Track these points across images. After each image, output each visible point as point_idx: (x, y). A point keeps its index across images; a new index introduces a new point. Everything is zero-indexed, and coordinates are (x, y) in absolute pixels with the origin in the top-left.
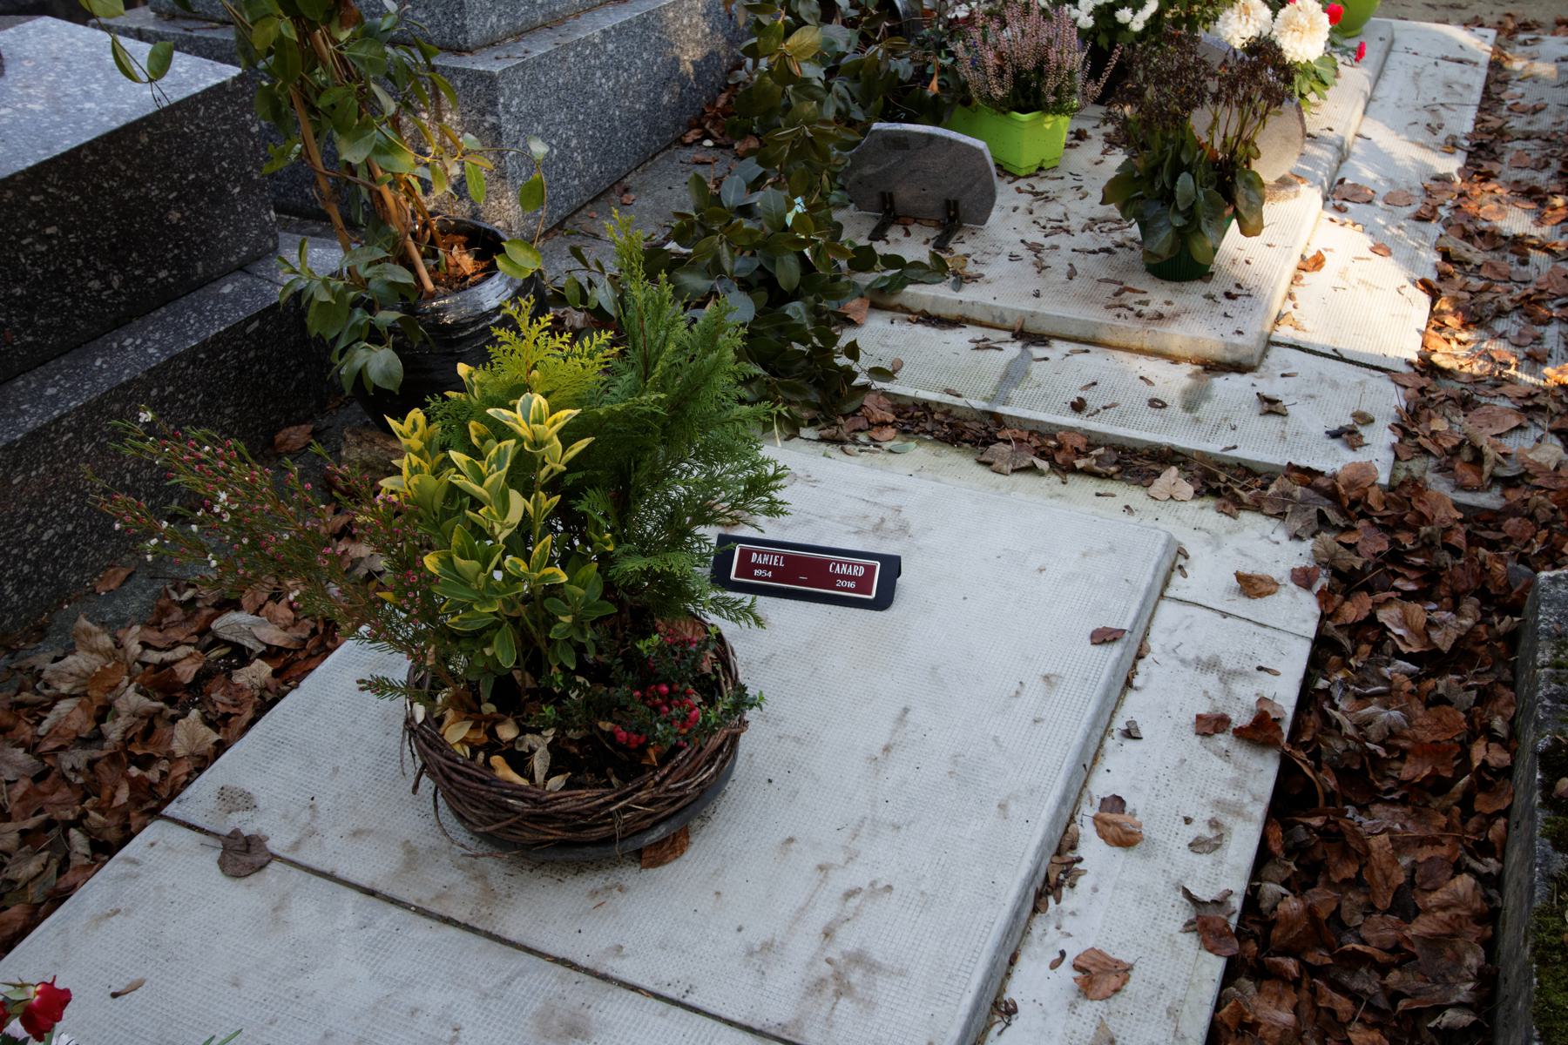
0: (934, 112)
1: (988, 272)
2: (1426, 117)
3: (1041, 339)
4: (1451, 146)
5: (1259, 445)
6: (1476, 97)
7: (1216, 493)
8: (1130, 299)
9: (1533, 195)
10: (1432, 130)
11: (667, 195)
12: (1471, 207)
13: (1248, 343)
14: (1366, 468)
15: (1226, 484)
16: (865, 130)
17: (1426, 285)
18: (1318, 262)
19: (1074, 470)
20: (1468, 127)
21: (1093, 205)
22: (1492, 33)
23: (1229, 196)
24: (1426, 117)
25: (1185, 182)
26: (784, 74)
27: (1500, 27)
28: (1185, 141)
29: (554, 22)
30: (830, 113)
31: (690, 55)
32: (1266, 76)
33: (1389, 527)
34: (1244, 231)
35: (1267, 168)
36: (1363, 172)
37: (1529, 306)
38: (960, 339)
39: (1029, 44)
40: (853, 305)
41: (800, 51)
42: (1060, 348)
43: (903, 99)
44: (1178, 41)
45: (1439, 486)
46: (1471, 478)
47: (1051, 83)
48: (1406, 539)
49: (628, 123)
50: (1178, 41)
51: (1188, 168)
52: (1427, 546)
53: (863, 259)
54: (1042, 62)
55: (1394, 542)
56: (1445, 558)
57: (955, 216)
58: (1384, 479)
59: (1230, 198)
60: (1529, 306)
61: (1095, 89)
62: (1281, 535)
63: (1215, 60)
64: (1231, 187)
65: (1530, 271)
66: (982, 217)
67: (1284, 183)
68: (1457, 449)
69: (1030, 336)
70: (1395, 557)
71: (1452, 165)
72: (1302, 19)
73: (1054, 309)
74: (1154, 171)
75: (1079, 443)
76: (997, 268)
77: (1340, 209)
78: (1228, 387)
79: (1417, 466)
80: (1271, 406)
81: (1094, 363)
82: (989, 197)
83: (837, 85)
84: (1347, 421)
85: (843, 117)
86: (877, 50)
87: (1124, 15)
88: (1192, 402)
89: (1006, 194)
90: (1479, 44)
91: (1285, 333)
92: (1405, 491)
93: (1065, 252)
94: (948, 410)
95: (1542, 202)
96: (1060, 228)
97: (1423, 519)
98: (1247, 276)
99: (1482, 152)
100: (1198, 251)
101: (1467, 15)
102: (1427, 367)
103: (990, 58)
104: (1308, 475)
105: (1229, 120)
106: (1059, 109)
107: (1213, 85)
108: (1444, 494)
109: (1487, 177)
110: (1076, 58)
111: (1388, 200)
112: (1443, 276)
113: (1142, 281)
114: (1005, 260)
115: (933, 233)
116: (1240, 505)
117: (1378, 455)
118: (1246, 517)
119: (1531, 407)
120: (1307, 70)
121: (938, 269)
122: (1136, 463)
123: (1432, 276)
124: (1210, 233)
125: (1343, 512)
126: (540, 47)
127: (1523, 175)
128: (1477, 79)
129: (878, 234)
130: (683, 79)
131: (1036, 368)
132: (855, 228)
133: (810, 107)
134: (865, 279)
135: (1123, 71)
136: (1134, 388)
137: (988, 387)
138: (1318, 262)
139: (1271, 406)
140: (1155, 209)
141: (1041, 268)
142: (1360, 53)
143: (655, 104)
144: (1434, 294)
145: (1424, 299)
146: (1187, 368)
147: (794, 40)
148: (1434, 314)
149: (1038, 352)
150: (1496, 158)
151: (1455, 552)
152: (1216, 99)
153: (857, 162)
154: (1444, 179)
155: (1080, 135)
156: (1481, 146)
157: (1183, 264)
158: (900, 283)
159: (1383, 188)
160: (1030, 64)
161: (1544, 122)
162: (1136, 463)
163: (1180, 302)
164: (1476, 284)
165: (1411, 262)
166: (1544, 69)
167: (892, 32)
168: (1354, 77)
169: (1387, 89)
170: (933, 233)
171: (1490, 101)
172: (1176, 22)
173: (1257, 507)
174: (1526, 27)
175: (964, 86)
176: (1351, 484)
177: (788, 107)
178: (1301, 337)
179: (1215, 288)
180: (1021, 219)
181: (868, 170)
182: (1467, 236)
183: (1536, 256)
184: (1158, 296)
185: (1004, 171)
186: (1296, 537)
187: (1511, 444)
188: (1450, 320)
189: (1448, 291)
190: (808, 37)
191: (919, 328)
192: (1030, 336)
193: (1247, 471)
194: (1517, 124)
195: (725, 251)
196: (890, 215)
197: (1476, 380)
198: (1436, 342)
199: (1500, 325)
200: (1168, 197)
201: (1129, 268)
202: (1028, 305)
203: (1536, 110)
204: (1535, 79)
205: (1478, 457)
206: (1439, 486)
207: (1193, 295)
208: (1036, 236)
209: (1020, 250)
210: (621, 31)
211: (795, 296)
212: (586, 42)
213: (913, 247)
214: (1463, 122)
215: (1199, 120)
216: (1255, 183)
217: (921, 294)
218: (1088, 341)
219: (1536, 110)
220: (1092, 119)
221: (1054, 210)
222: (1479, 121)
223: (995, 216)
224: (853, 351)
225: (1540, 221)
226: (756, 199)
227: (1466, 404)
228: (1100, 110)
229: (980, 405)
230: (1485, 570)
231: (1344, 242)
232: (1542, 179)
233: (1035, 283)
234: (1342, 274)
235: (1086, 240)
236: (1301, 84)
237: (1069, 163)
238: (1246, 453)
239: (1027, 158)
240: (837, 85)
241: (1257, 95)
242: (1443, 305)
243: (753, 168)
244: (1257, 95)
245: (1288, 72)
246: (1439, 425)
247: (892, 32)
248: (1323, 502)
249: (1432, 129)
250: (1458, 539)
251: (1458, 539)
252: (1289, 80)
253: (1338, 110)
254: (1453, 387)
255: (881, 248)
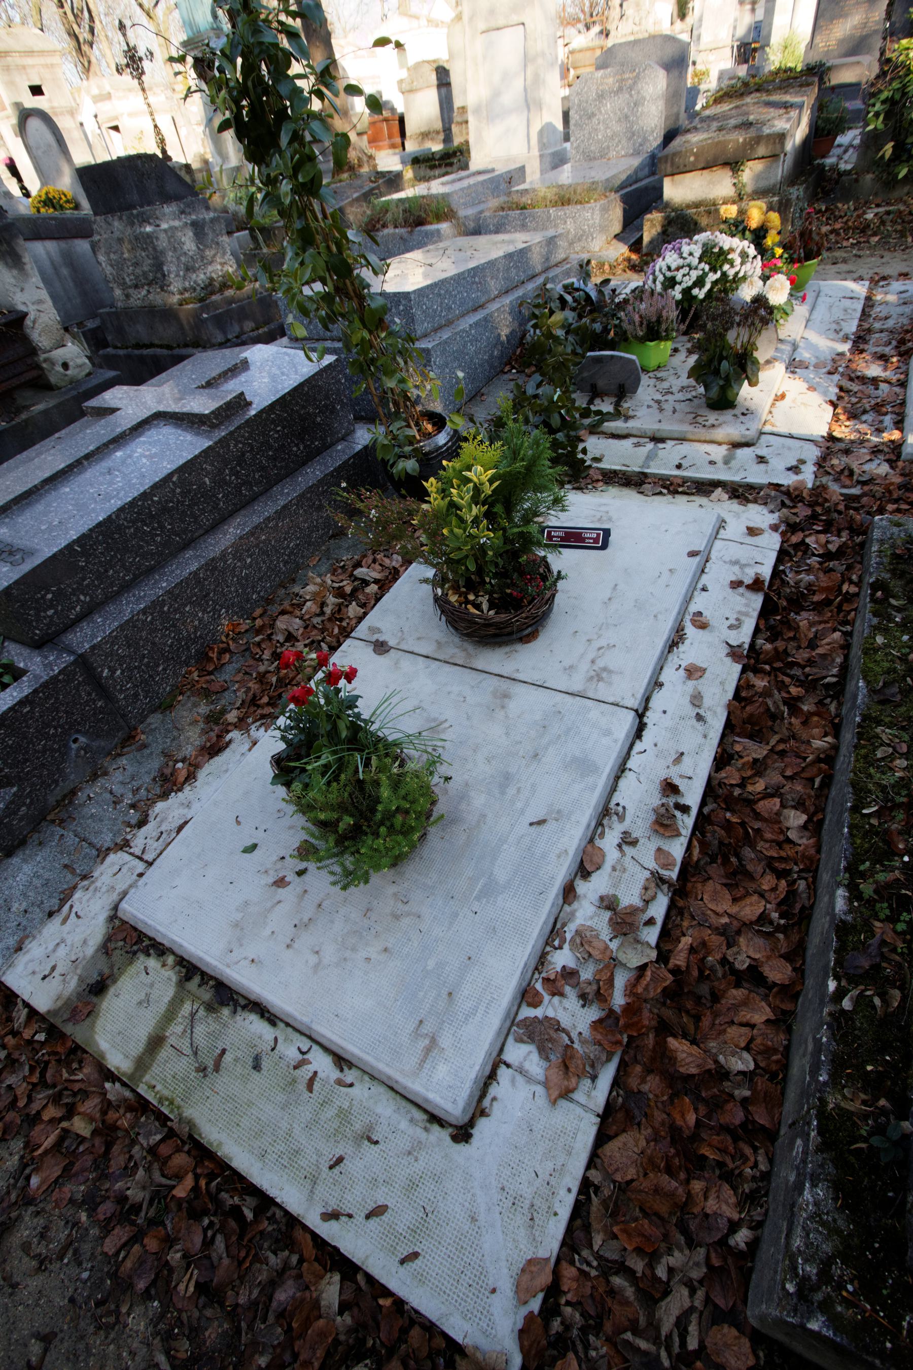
0: (612, 346)
1: (638, 414)
2: (834, 326)
3: (662, 440)
4: (846, 338)
5: (757, 476)
6: (858, 314)
7: (737, 497)
8: (700, 419)
9: (883, 358)
10: (837, 332)
11: (500, 398)
12: (853, 366)
13: (751, 434)
14: (802, 482)
15: (741, 493)
16: (583, 356)
17: (832, 403)
18: (783, 396)
19: (678, 493)
20: (854, 329)
21: (684, 380)
22: (867, 283)
23: (744, 369)
24: (834, 326)
25: (725, 365)
26: (549, 335)
27: (871, 280)
28: (725, 346)
29: (449, 323)
30: (569, 350)
31: (504, 332)
32: (761, 312)
33: (811, 505)
34: (750, 385)
35: (761, 355)
36: (804, 354)
37: (878, 408)
38: (627, 443)
39: (653, 310)
40: (582, 433)
41: (555, 324)
42: (670, 443)
43: (599, 341)
44: (722, 300)
45: (834, 487)
46: (848, 482)
47: (664, 327)
48: (819, 510)
49: (481, 365)
50: (722, 300)
51: (726, 358)
52: (828, 511)
53: (586, 413)
54: (660, 317)
55: (814, 511)
56: (836, 515)
57: (623, 390)
58: (810, 485)
59: (745, 371)
60: (878, 408)
61: (683, 327)
62: (765, 511)
63: (738, 308)
64: (744, 365)
65: (880, 392)
66: (634, 390)
67: (768, 362)
68: (842, 471)
69: (657, 439)
70: (814, 517)
71: (845, 347)
72: (777, 285)
73: (668, 426)
74: (711, 361)
75: (680, 481)
76: (642, 412)
77: (793, 372)
78: (741, 453)
79: (824, 480)
80: (761, 460)
81: (685, 448)
82: (638, 380)
83: (570, 338)
84: (794, 463)
85: (574, 352)
86: (586, 320)
87: (695, 291)
88: (727, 461)
89: (645, 380)
90: (860, 289)
91: (768, 428)
92: (819, 490)
93: (671, 402)
94: (624, 473)
95: (887, 361)
96: (669, 392)
97: (826, 500)
98: (752, 405)
99: (860, 341)
100: (730, 395)
101: (856, 275)
102: (831, 438)
103: (637, 318)
104: (777, 487)
105: (744, 333)
106: (667, 338)
107: (737, 319)
108: (835, 490)
109: (862, 351)
110: (674, 314)
111: (816, 366)
112: (839, 398)
113: (705, 412)
114: (645, 409)
115: (614, 400)
116: (748, 501)
117: (808, 477)
118: (751, 506)
119: (876, 451)
120: (779, 308)
121: (617, 414)
122: (704, 488)
123: (834, 398)
124: (735, 387)
125: (792, 500)
126: (446, 335)
127: (878, 349)
128: (859, 306)
129: (591, 402)
130: (502, 343)
131: (660, 452)
132: (581, 400)
133: (560, 349)
134: (587, 421)
135: (697, 316)
136: (703, 456)
137: (640, 462)
138: (783, 396)
139: (761, 460)
140: (712, 378)
141: (661, 410)
142: (804, 298)
143: (491, 356)
144: (834, 405)
145: (830, 409)
146: (725, 447)
147: (553, 318)
148: (835, 415)
149: (661, 446)
150: (866, 342)
151: (840, 513)
152: (739, 325)
153: (580, 373)
154: (842, 354)
155: (676, 350)
156: (859, 337)
157: (723, 402)
158: (601, 422)
159: (813, 361)
160: (654, 319)
161: (890, 324)
162: (704, 488)
163: (722, 419)
164: (854, 400)
165: (825, 393)
166: (892, 298)
167: (591, 312)
168: (801, 310)
169: (817, 315)
170: (614, 400)
171: (865, 315)
172: (720, 291)
173: (755, 501)
174: (884, 278)
175: (625, 332)
176: (796, 489)
177: (550, 350)
178: (775, 430)
179: (737, 411)
180: (651, 390)
181: (585, 374)
182: (851, 379)
183: (883, 386)
184: (712, 417)
185: (645, 370)
186: (772, 512)
187: (866, 467)
188: (842, 417)
189: (841, 404)
190: (558, 317)
191: (611, 441)
192: (657, 439)
193: (751, 487)
194: (877, 325)
195: (530, 414)
196: (595, 393)
197: (852, 442)
198: (835, 427)
199: (864, 418)
200: (717, 372)
201: (699, 407)
202: (656, 426)
203: (886, 318)
204: (886, 303)
205: (851, 473)
206: (834, 487)
207: (727, 415)
208: (658, 397)
209: (652, 403)
210: (477, 324)
211: (559, 431)
212: (464, 331)
213: (606, 406)
214: (852, 327)
215: (731, 336)
216: (755, 362)
217: (611, 426)
218: (682, 439)
219: (886, 318)
220: (684, 344)
221: (665, 385)
222: (859, 326)
223: (640, 390)
224: (584, 451)
225: (885, 369)
226: (540, 391)
227: (847, 452)
228: (685, 338)
229: (637, 469)
230: (852, 519)
231: (795, 387)
232: (887, 350)
233: (659, 416)
234: (794, 401)
235: (680, 396)
236: (777, 315)
237: (672, 363)
238: (752, 479)
239: (653, 363)
240: (570, 338)
241: (757, 322)
242: (839, 410)
243: (537, 377)
244: (757, 322)
245: (771, 310)
246: (835, 462)
247: (591, 312)
248: (784, 497)
249: (837, 332)
250: (841, 507)
251: (841, 507)
252: (771, 313)
253: (792, 328)
254: (842, 446)
255: (593, 408)
